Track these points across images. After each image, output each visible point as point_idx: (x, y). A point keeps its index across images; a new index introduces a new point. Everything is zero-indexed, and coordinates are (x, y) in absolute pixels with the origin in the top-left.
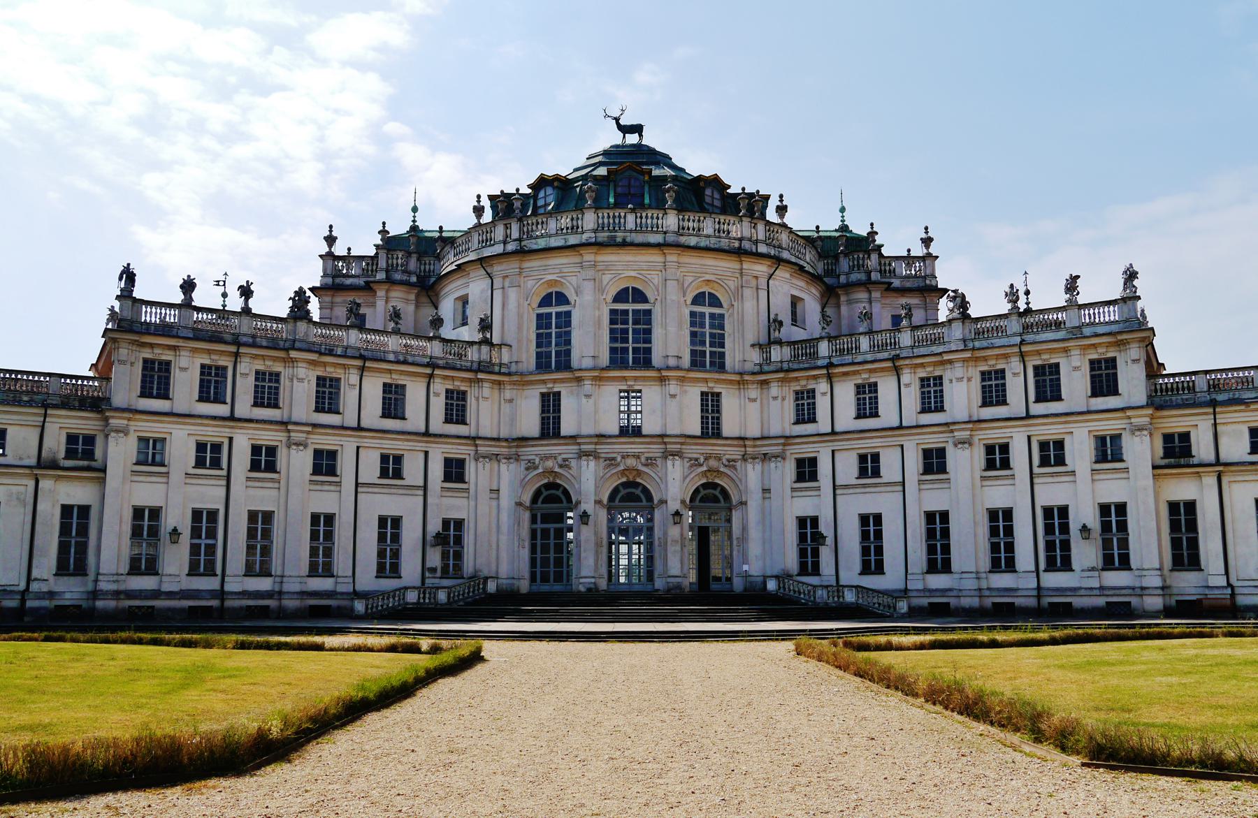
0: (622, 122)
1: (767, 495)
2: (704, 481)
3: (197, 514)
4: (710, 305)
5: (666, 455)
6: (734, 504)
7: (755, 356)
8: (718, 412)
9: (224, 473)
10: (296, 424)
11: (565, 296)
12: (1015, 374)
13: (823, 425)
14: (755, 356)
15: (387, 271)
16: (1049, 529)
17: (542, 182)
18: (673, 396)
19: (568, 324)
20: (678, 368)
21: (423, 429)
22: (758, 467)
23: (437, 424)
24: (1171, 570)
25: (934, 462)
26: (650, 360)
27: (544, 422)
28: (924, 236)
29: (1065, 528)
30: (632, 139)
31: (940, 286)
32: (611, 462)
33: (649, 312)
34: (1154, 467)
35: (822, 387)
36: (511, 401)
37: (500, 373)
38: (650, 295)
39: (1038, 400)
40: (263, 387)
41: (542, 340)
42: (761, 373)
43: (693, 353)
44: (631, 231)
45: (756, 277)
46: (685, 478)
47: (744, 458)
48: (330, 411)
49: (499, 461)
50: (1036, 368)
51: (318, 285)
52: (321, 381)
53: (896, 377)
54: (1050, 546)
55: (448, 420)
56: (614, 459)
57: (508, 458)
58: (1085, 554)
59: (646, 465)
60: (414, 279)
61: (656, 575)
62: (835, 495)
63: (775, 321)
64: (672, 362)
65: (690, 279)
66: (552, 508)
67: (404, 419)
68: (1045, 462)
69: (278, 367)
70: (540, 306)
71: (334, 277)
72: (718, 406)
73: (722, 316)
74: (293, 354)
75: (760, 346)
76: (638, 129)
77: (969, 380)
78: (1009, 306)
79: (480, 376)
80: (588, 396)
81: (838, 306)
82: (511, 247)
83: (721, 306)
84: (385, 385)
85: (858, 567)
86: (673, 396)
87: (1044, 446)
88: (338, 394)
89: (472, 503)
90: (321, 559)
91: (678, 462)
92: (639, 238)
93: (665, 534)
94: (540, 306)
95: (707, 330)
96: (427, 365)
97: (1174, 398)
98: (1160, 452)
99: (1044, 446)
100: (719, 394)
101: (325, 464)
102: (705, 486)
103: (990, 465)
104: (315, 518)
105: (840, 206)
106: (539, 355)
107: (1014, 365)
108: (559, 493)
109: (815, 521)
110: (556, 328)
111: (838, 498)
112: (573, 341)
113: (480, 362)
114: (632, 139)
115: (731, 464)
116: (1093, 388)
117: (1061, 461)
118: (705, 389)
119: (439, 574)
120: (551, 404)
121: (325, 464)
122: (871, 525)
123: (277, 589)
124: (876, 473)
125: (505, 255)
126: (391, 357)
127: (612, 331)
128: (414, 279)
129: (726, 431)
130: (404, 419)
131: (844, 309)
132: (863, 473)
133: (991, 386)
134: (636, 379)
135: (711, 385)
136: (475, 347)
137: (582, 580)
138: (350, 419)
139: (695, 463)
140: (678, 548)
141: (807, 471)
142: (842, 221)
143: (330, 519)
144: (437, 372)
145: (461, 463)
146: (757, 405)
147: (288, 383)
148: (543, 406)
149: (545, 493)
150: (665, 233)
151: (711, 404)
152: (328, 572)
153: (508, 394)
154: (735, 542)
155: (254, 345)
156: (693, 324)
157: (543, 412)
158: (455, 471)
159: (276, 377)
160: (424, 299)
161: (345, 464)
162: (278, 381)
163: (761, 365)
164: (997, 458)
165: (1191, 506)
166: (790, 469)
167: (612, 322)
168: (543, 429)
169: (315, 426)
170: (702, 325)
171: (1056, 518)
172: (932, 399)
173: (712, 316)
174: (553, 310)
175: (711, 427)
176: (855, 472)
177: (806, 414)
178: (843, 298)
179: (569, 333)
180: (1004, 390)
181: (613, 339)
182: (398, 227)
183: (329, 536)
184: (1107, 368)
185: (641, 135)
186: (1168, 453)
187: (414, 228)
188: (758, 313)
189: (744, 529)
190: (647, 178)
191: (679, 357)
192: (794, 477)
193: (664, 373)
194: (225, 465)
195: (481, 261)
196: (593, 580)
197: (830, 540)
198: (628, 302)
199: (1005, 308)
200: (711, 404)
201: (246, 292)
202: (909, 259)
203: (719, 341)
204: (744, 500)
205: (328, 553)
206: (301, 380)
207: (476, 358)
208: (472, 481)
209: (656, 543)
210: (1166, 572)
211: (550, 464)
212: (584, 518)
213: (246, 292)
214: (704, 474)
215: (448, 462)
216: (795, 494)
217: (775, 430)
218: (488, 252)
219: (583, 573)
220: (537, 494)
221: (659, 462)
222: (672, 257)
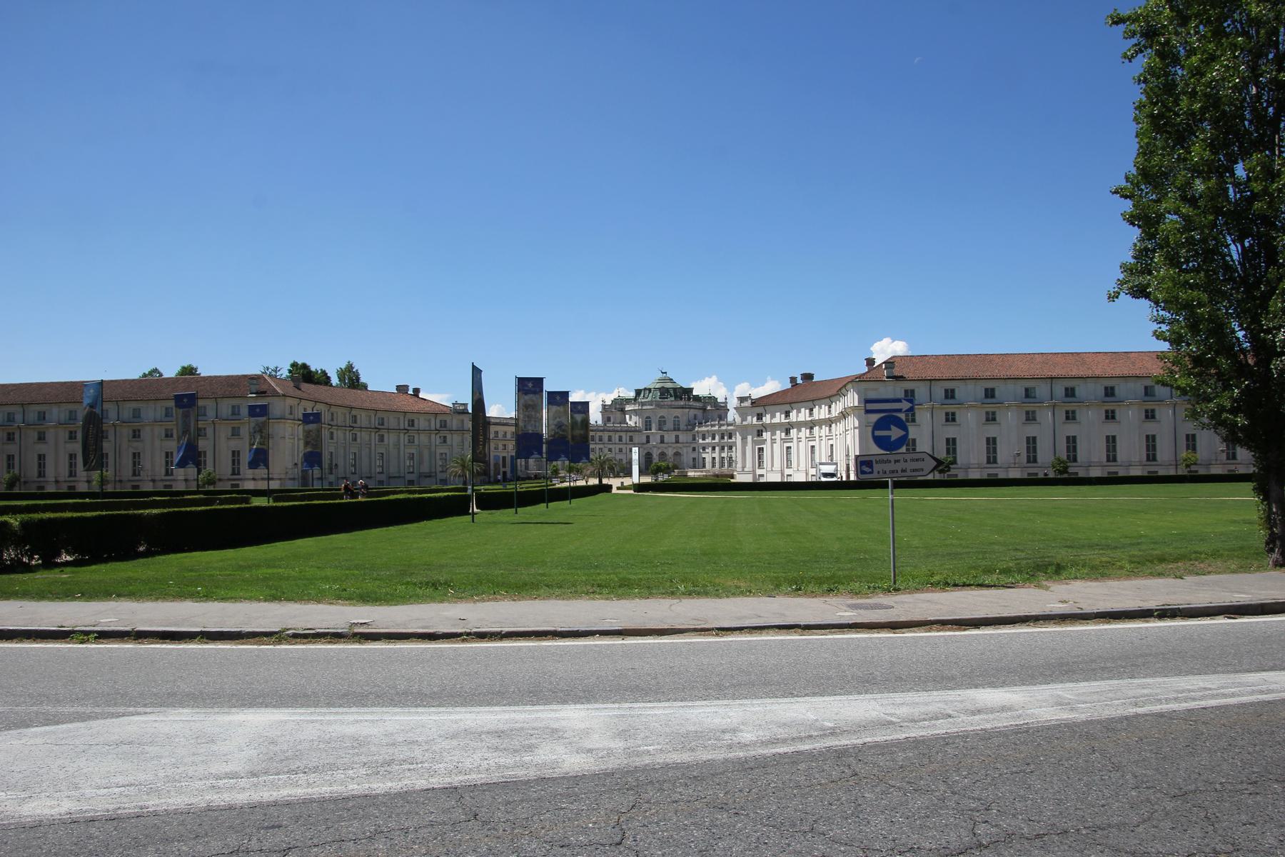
17: (645, 389)
23: (628, 442)
32: (659, 448)
41: (646, 425)
76: (666, 373)
114: (665, 375)
120: (648, 437)
129: (680, 441)
141: (694, 449)
151: (677, 437)
159: (601, 436)
161: (613, 450)
164: (723, 448)
175: (677, 442)
177: (694, 439)
195: (634, 410)
200: (677, 437)
201: (596, 422)
203: (679, 425)
213: (596, 422)
217: (689, 441)
218: (636, 408)
222: (670, 410)
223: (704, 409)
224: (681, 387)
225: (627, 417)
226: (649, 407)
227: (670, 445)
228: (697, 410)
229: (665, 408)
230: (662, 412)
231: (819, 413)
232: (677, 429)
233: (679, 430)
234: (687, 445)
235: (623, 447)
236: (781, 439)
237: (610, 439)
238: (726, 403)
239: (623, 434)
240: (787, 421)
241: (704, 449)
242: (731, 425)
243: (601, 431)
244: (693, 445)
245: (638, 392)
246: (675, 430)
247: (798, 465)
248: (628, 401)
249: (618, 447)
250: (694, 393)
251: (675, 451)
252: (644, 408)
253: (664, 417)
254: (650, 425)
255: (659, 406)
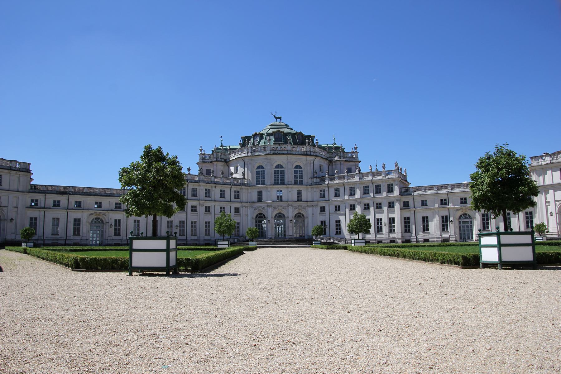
0: (277, 116)
1: (313, 215)
2: (298, 212)
3: (180, 222)
4: (299, 168)
5: (288, 206)
6: (305, 217)
7: (310, 181)
8: (301, 195)
9: (186, 212)
10: (201, 200)
11: (263, 167)
12: (371, 187)
14: (310, 181)
15: (216, 158)
16: (378, 224)
17: (255, 135)
18: (290, 192)
19: (264, 174)
20: (291, 185)
21: (230, 201)
22: (311, 208)
24: (405, 233)
26: (284, 182)
27: (258, 198)
28: (355, 147)
29: (381, 223)
31: (359, 160)
32: (275, 208)
33: (284, 171)
34: (401, 209)
35: (327, 189)
36: (250, 193)
37: (247, 186)
38: (284, 166)
39: (376, 193)
40: (193, 192)
42: (312, 185)
43: (295, 180)
44: (279, 150)
45: (311, 161)
46: (293, 211)
47: (308, 206)
48: (208, 197)
49: (248, 208)
50: (376, 185)
51: (198, 162)
52: (206, 190)
53: (344, 187)
54: (378, 227)
55: (235, 198)
56: (276, 207)
57: (250, 207)
58: (385, 229)
59: (283, 208)
60: (223, 160)
61: (286, 235)
62: (329, 215)
63: (315, 172)
64: (289, 183)
65: (294, 162)
66: (260, 219)
67: (225, 198)
68: (377, 208)
69: (196, 187)
70: (257, 169)
71: (202, 159)
72: (301, 194)
73: (302, 171)
74: (200, 184)
75: (311, 178)
76: (280, 118)
77: (360, 188)
78: (370, 170)
79: (243, 187)
80: (269, 192)
81: (332, 165)
82: (250, 154)
83: (302, 168)
84: (220, 190)
85: (335, 233)
86: (290, 192)
87: (377, 204)
88: (210, 193)
89: (241, 218)
90: (207, 232)
91: (291, 208)
92: (281, 152)
93: (288, 225)
94: (257, 169)
95: (298, 175)
96: (231, 185)
97: (406, 193)
98: (402, 205)
99: (377, 204)
100: (301, 191)
101: (208, 210)
102: (298, 213)
103: (365, 208)
104: (206, 223)
105: (334, 138)
106: (257, 181)
107: (370, 185)
108: (262, 215)
109: (325, 222)
110: (261, 174)
111: (330, 216)
112: (265, 178)
113: (242, 184)
114: (279, 120)
115: (304, 208)
116: (388, 191)
117: (381, 208)
118: (298, 190)
119: (234, 235)
120: (260, 194)
121: (208, 210)
122: (338, 223)
123: (198, 239)
124: (339, 210)
125: (248, 156)
126: (222, 183)
127: (275, 175)
128: (223, 160)
129: (303, 201)
130: (225, 198)
131: (334, 166)
132: (336, 210)
133: (365, 190)
134: (281, 188)
135: (299, 188)
136: (241, 180)
137: (268, 237)
138: (213, 198)
139: (296, 208)
140: (292, 229)
141: (323, 210)
142: (334, 142)
143: (209, 223)
144: (233, 186)
145: (238, 208)
146: (311, 193)
147: (199, 190)
148: (258, 194)
149: (259, 216)
150: (288, 151)
151: (299, 193)
152: (209, 235)
153: (249, 191)
154: (305, 227)
155: (191, 182)
156: (295, 173)
157: (258, 195)
158: (237, 210)
159: (196, 189)
160: (226, 165)
161: (212, 210)
162: (196, 190)
163: (312, 183)
165: (409, 218)
166: (319, 209)
167: (275, 173)
168: (258, 200)
169: (205, 200)
170: (297, 173)
171: (379, 221)
173: (299, 171)
174: (260, 170)
175: (299, 199)
176: (334, 210)
177: (323, 196)
178: (334, 164)
179: (264, 176)
180: (368, 191)
181: (275, 177)
182: (218, 146)
183: (209, 226)
184: (391, 186)
185: (281, 120)
186: (404, 206)
187: (222, 146)
188: (311, 169)
189: (308, 224)
190: (283, 134)
191: (291, 182)
192: (320, 211)
193: (288, 186)
194: (186, 210)
196: (271, 237)
197: (328, 226)
198: (279, 168)
199: (369, 171)
200: (299, 193)
201: (189, 169)
203: (301, 177)
204: (307, 216)
205: (209, 230)
206: (202, 190)
207: (241, 182)
208: (241, 212)
209: (286, 227)
210: (403, 233)
211: (260, 208)
212: (269, 222)
213: (189, 169)
214: (298, 211)
215: (235, 208)
216: (320, 215)
217: (315, 199)
218: (243, 155)
219: (269, 235)
220: (257, 216)
221: (287, 207)
222: (289, 156)
223: (331, 162)
224: (300, 133)
225: (232, 169)
226: (260, 154)
227: (290, 203)
228: (322, 160)
229: (282, 154)
230: (279, 160)
232: (298, 181)
233: (301, 183)
234: (313, 204)
235: (226, 205)
237: (208, 193)
239: (227, 189)
241: (338, 208)
242: (380, 174)
243: (195, 182)
244: (322, 204)
246: (296, 183)
249: (219, 205)
251: (296, 212)
252: (256, 154)
253: (281, 167)
254: (263, 177)
255: (275, 152)
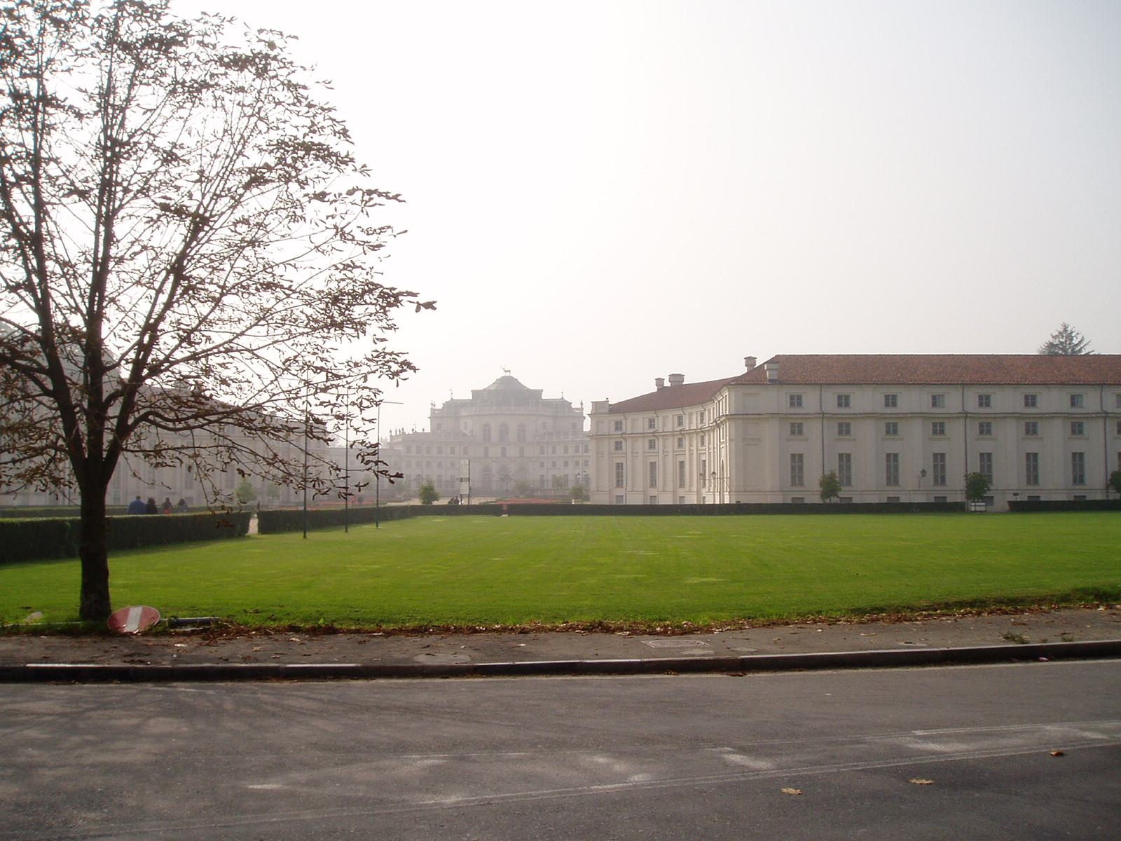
13: (545, 455)
25: (566, 464)
30: (508, 374)
76: (509, 371)
107: (580, 445)
141: (542, 465)
164: (577, 463)
172: (566, 451)
177: (542, 452)
182: (449, 399)
202: (577, 409)
231: (690, 423)
236: (644, 452)
238: (582, 409)
240: (652, 430)
245: (475, 393)
247: (665, 485)
248: (463, 404)
250: (544, 397)
